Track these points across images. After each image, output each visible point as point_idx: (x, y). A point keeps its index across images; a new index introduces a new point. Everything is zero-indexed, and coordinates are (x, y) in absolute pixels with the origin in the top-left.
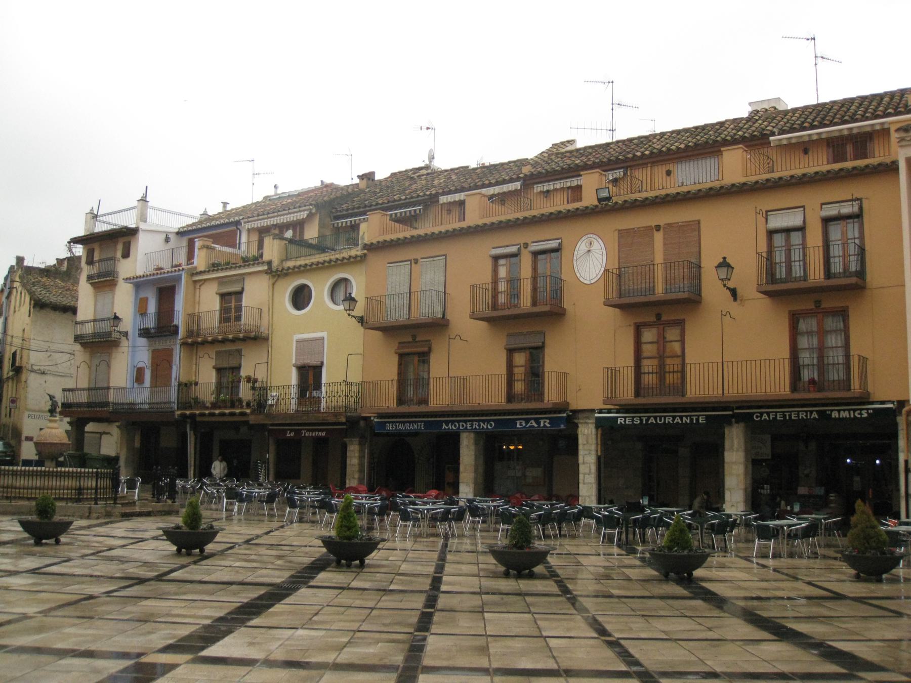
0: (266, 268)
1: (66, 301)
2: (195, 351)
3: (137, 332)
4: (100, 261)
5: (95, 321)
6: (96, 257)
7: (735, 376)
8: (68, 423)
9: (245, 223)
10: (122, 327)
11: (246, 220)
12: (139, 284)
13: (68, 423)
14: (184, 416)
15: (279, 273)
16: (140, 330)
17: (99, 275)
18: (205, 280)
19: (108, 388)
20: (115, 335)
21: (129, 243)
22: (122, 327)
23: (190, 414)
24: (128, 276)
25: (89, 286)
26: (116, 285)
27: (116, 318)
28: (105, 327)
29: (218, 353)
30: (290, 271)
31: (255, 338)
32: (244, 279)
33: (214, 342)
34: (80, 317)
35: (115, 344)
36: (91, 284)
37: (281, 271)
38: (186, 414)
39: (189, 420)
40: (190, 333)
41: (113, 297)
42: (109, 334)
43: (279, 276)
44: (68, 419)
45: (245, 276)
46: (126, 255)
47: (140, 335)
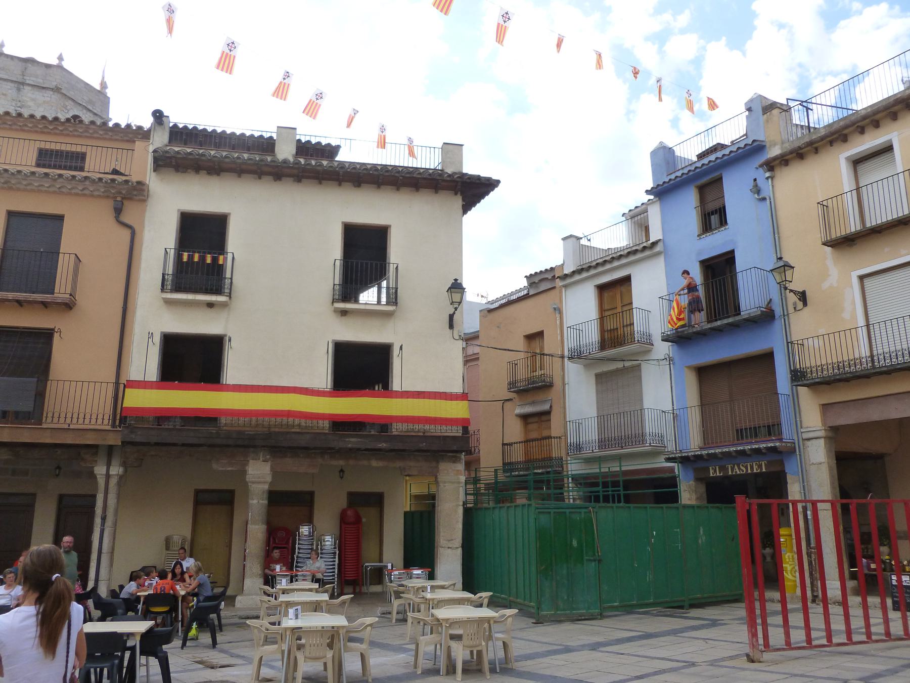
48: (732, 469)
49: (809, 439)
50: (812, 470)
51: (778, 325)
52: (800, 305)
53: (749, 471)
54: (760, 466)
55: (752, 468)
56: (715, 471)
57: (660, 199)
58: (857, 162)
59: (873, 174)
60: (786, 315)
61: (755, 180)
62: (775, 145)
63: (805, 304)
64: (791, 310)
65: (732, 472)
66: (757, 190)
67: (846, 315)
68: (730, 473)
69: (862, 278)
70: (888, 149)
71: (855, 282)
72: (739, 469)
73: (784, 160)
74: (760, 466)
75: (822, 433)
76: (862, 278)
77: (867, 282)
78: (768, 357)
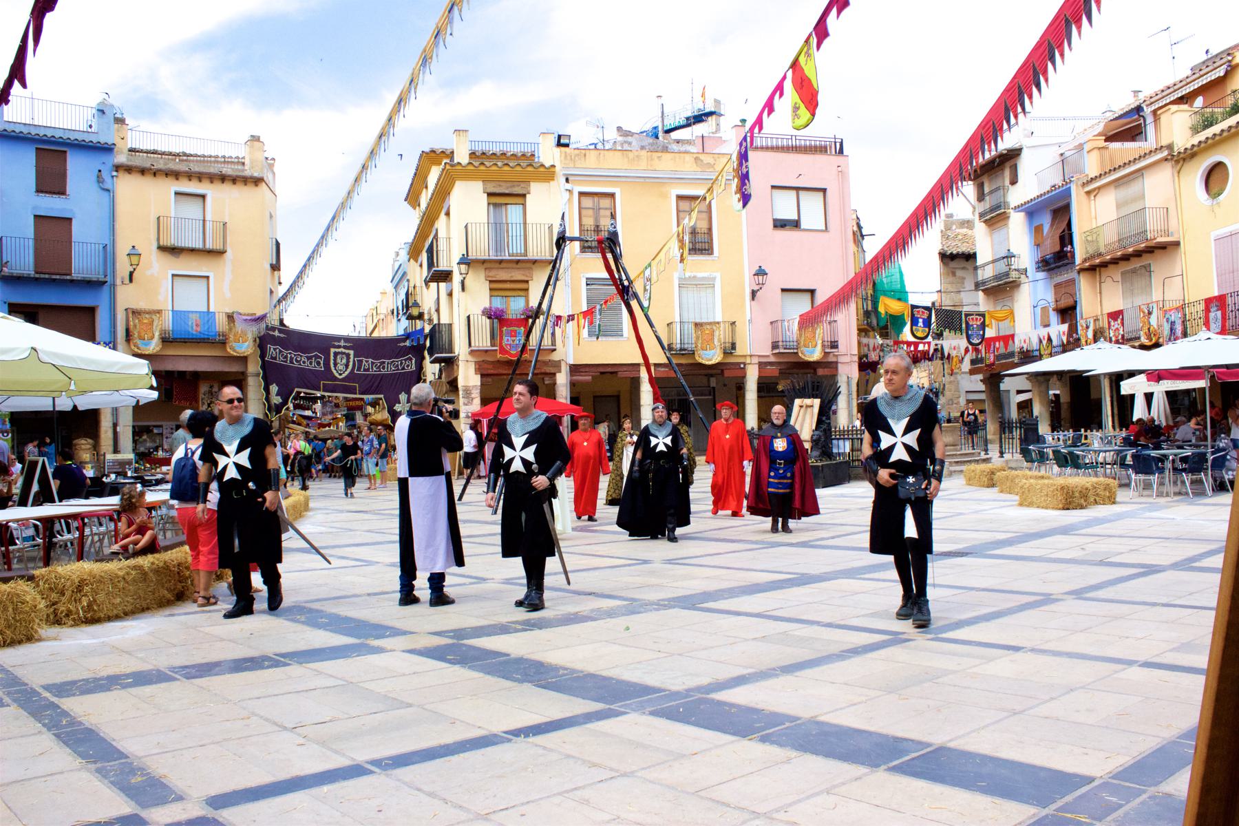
0: (1165, 153)
1: (963, 248)
2: (1098, 277)
3: (1034, 266)
4: (991, 192)
5: (994, 261)
6: (987, 190)
8: (981, 381)
9: (1147, 106)
10: (1016, 264)
11: (1148, 102)
12: (1032, 211)
13: (981, 381)
15: (1182, 156)
16: (1037, 263)
17: (992, 210)
18: (1099, 188)
20: (1014, 275)
21: (1016, 166)
22: (1016, 264)
25: (983, 225)
26: (1009, 217)
28: (1002, 267)
29: (1122, 274)
30: (1195, 149)
31: (1163, 247)
32: (1143, 174)
34: (980, 262)
35: (1014, 285)
37: (1185, 152)
41: (1008, 232)
42: (1007, 274)
43: (1184, 160)
44: (980, 377)
45: (1144, 172)
46: (1014, 182)
47: (1038, 269)
51: (106, 290)
52: (127, 281)
58: (177, 193)
59: (191, 210)
60: (114, 285)
61: (100, 171)
62: (122, 153)
63: (131, 280)
64: (118, 282)
66: (100, 179)
67: (161, 298)
69: (173, 275)
70: (203, 197)
73: (129, 169)
76: (173, 275)
77: (175, 278)
78: (91, 311)
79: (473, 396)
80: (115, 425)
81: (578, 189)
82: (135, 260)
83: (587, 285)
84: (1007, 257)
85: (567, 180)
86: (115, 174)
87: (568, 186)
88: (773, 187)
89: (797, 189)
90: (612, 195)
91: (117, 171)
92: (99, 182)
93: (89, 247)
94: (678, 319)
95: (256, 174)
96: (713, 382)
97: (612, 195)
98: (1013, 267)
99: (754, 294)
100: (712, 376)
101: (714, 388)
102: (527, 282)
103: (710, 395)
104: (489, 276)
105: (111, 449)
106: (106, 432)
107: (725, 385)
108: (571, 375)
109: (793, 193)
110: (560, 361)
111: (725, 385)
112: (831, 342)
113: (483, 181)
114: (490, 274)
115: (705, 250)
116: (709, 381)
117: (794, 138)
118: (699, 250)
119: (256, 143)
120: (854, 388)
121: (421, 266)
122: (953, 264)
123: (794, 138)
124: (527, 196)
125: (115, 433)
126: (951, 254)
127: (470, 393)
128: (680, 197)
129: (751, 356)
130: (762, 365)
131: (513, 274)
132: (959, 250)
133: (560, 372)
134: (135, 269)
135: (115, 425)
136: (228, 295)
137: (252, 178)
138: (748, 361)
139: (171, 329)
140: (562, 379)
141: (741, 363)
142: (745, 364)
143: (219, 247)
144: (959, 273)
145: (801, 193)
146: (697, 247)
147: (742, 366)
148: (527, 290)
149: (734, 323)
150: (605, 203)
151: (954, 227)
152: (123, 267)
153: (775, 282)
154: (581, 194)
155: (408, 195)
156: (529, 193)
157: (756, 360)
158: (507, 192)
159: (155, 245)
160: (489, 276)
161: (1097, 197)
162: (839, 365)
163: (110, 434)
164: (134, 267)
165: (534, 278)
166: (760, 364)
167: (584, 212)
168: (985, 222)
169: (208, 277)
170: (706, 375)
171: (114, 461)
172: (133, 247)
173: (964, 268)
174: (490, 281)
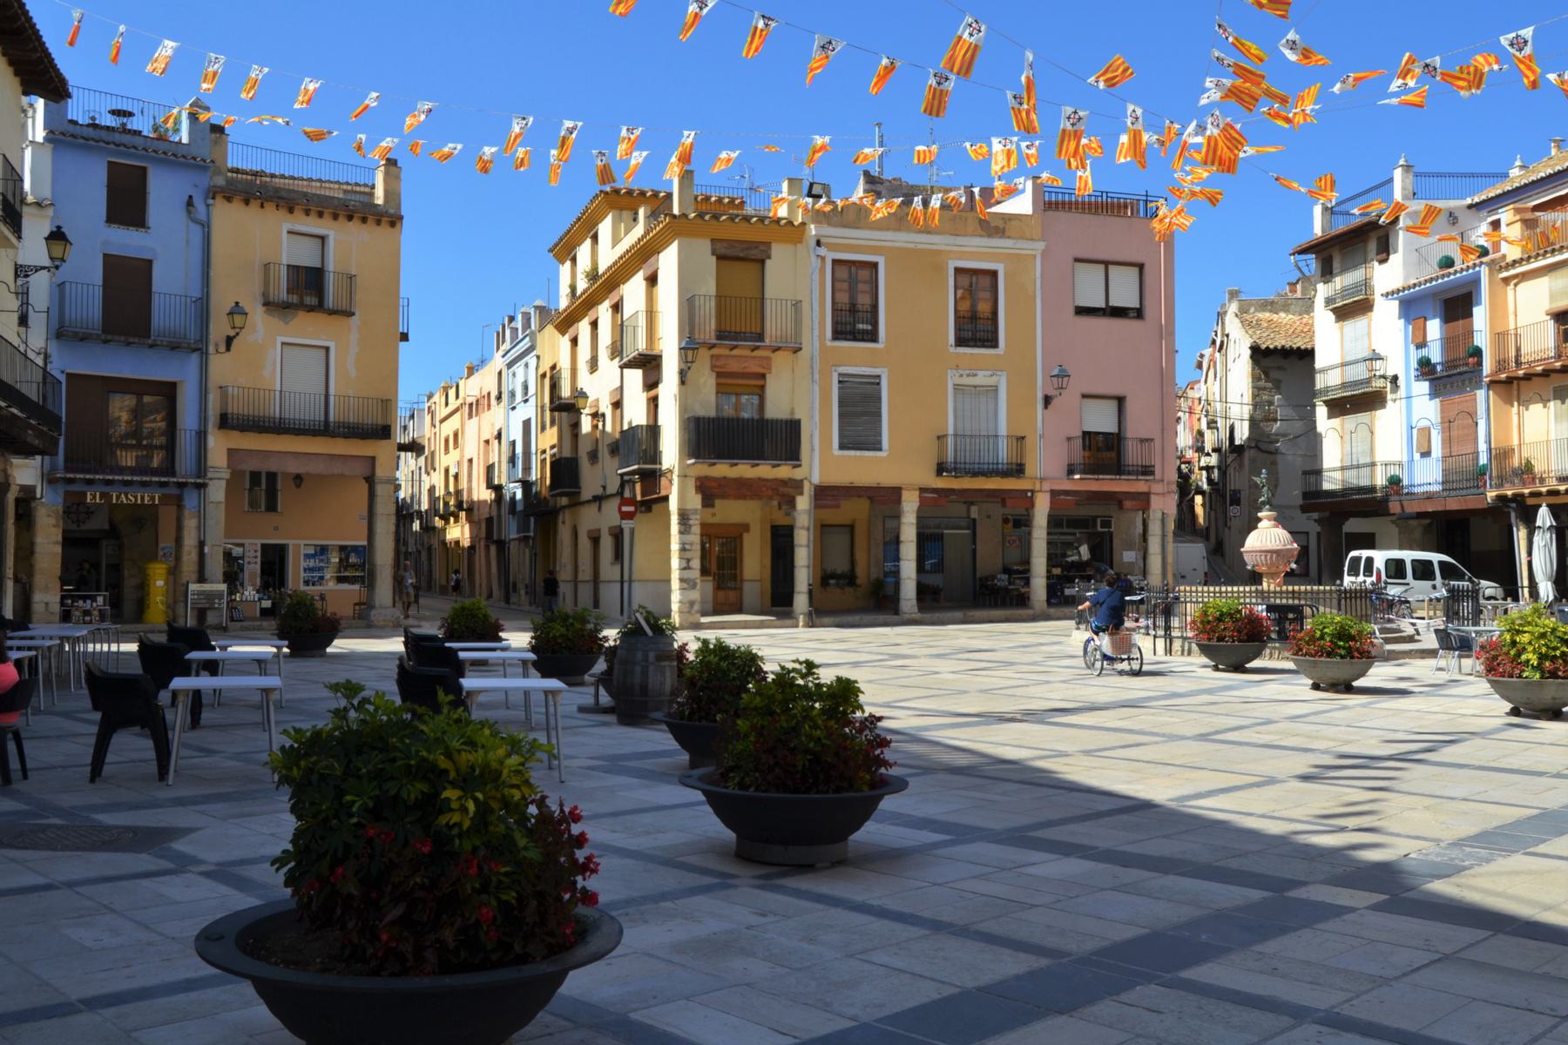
1: (1299, 343)
7: (743, 311)
14: (1502, 499)
19: (1373, 464)
20: (1379, 384)
23: (1514, 495)
24: (1390, 290)
27: (1376, 357)
28: (1359, 372)
33: (1546, 373)
36: (1331, 310)
38: (1506, 496)
39: (1514, 505)
40: (1501, 364)
41: (1369, 326)
42: (1368, 381)
48: (118, 497)
49: (211, 479)
50: (210, 508)
52: (222, 348)
53: (139, 502)
54: (153, 498)
55: (143, 498)
56: (94, 497)
57: (54, 149)
63: (228, 348)
64: (211, 349)
65: (117, 500)
68: (114, 501)
71: (279, 345)
72: (127, 498)
74: (153, 498)
75: (227, 476)
76: (283, 344)
79: (691, 522)
80: (201, 544)
81: (830, 256)
82: (238, 319)
83: (840, 382)
84: (1371, 359)
85: (818, 243)
86: (210, 201)
87: (822, 251)
88: (1077, 260)
89: (1106, 264)
90: (875, 265)
91: (213, 198)
92: (189, 212)
93: (167, 300)
94: (951, 431)
95: (392, 211)
96: (974, 512)
97: (875, 265)
98: (1378, 373)
99: (1047, 400)
100: (972, 503)
101: (974, 520)
102: (763, 376)
103: (968, 528)
104: (715, 366)
105: (194, 576)
106: (189, 554)
107: (989, 517)
108: (816, 499)
109: (1102, 267)
110: (802, 481)
111: (989, 517)
112: (1142, 466)
113: (712, 240)
114: (718, 364)
115: (988, 340)
116: (968, 511)
117: (1104, 195)
118: (980, 340)
119: (393, 169)
120: (1171, 526)
121: (574, 341)
122: (1266, 362)
123: (1104, 195)
124: (768, 262)
125: (201, 555)
126: (1267, 348)
127: (688, 519)
128: (958, 271)
129: (1042, 479)
130: (1054, 494)
131: (746, 364)
132: (1277, 344)
133: (801, 493)
134: (237, 334)
135: (201, 544)
136: (353, 373)
137: (386, 214)
138: (1038, 487)
139: (277, 415)
140: (803, 503)
141: (1028, 491)
142: (1033, 492)
143: (344, 306)
144: (1274, 374)
145: (1111, 268)
146: (978, 336)
147: (1029, 494)
148: (763, 387)
149: (1023, 438)
150: (864, 274)
151: (1252, 310)
152: (219, 328)
153: (1076, 386)
154: (835, 262)
155: (556, 245)
156: (769, 257)
157: (1047, 486)
158: (741, 255)
159: (260, 300)
160: (715, 366)
161: (1518, 288)
162: (1152, 497)
163: (194, 556)
164: (238, 330)
165: (774, 370)
166: (1054, 493)
167: (837, 284)
168: (1334, 311)
169: (327, 349)
170: (965, 503)
171: (199, 593)
172: (237, 303)
173: (1280, 368)
174: (719, 375)
